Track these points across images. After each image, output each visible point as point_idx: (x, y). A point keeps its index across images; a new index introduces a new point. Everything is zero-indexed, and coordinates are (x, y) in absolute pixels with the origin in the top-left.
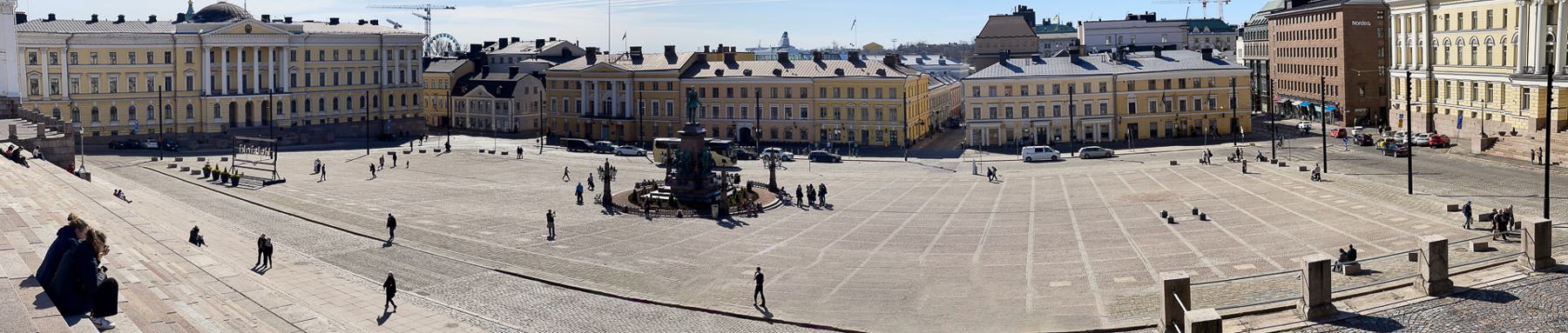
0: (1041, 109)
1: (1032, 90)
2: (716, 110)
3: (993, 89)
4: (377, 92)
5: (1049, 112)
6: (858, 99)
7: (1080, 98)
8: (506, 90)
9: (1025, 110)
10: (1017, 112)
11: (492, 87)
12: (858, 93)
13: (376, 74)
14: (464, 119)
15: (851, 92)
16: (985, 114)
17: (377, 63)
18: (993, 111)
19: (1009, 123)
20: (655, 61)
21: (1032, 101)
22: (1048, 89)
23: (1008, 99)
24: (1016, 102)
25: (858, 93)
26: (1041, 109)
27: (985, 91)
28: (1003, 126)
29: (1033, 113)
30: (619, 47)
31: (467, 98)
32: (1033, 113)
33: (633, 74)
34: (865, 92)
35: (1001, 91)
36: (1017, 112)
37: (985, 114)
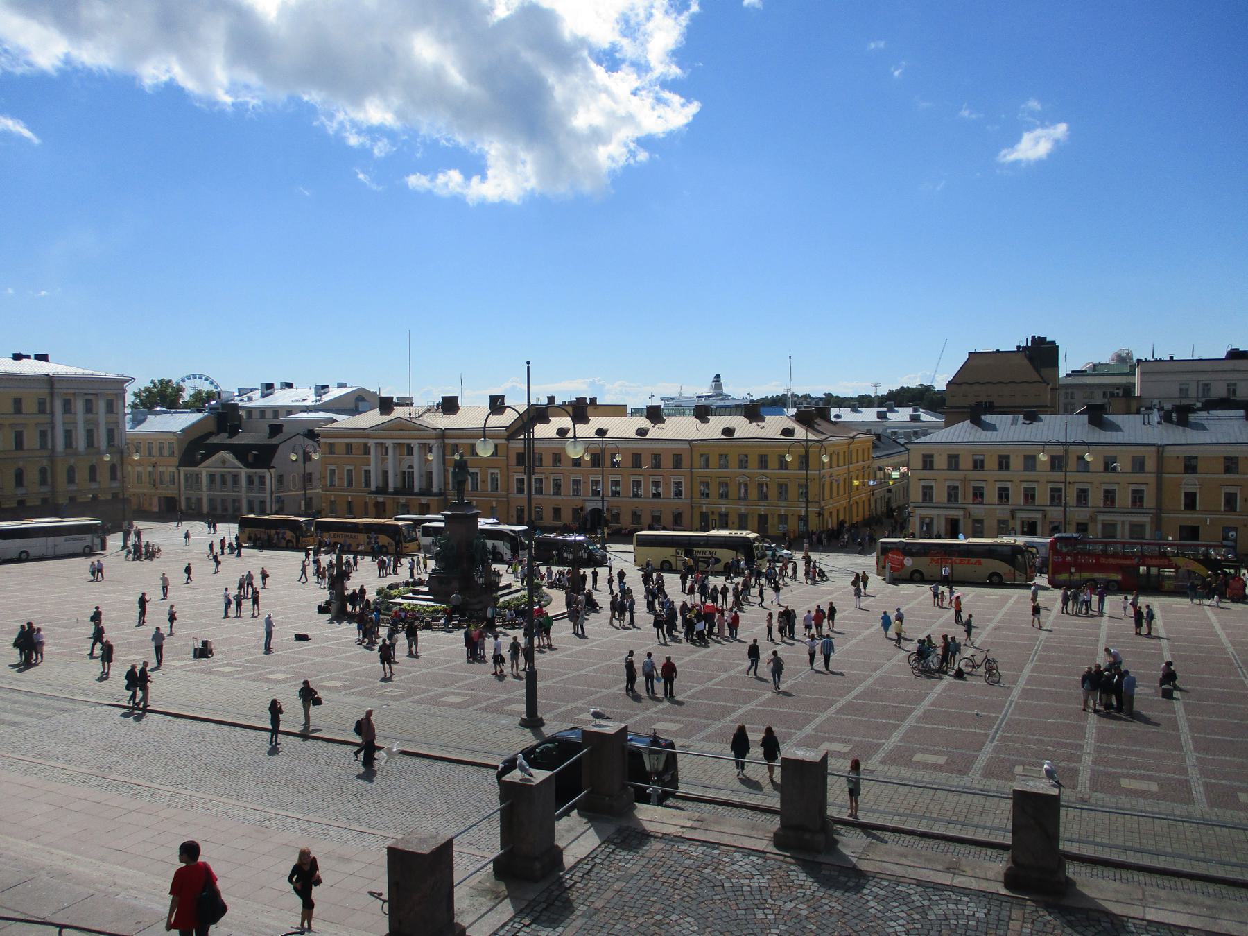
1: (1016, 463)
2: (557, 486)
3: (953, 462)
4: (45, 463)
5: (1043, 497)
8: (260, 456)
9: (1004, 495)
10: (991, 494)
11: (241, 452)
13: (43, 434)
14: (199, 500)
16: (940, 495)
17: (44, 418)
18: (953, 493)
20: (472, 415)
21: (1016, 480)
23: (977, 474)
24: (991, 481)
27: (940, 462)
28: (968, 514)
29: (1017, 498)
30: (425, 396)
31: (203, 470)
32: (1017, 498)
33: (443, 434)
35: (966, 463)
36: (991, 494)
37: (940, 495)
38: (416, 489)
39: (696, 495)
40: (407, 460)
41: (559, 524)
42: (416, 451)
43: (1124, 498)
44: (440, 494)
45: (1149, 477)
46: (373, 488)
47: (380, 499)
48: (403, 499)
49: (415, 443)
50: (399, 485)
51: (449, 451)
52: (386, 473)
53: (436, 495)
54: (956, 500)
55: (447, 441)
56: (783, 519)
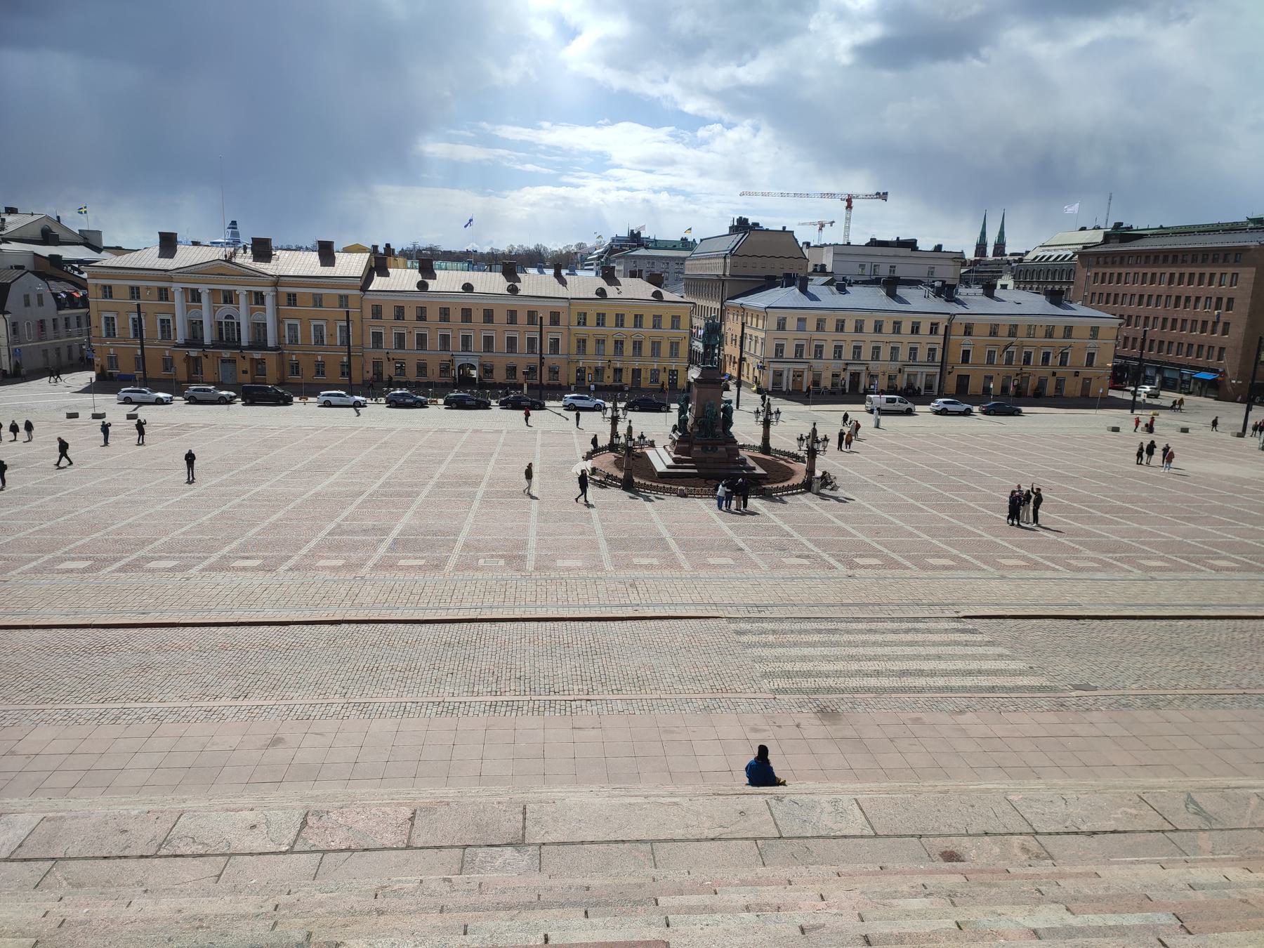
0: (857, 349)
1: (850, 326)
5: (866, 354)
6: (629, 329)
7: (959, 341)
9: (838, 350)
10: (828, 351)
12: (629, 321)
15: (620, 320)
18: (799, 348)
19: (818, 364)
21: (848, 338)
22: (869, 326)
23: (819, 335)
24: (829, 339)
25: (629, 321)
26: (857, 349)
29: (847, 354)
32: (847, 354)
34: (638, 320)
36: (828, 351)
38: (244, 343)
39: (574, 349)
40: (228, 309)
41: (424, 380)
42: (242, 299)
43: (922, 355)
44: (276, 349)
45: (939, 339)
46: (182, 342)
47: (194, 353)
48: (226, 354)
49: (241, 290)
50: (216, 337)
51: (284, 300)
52: (195, 327)
53: (272, 349)
54: (801, 356)
55: (280, 289)
56: (655, 373)
